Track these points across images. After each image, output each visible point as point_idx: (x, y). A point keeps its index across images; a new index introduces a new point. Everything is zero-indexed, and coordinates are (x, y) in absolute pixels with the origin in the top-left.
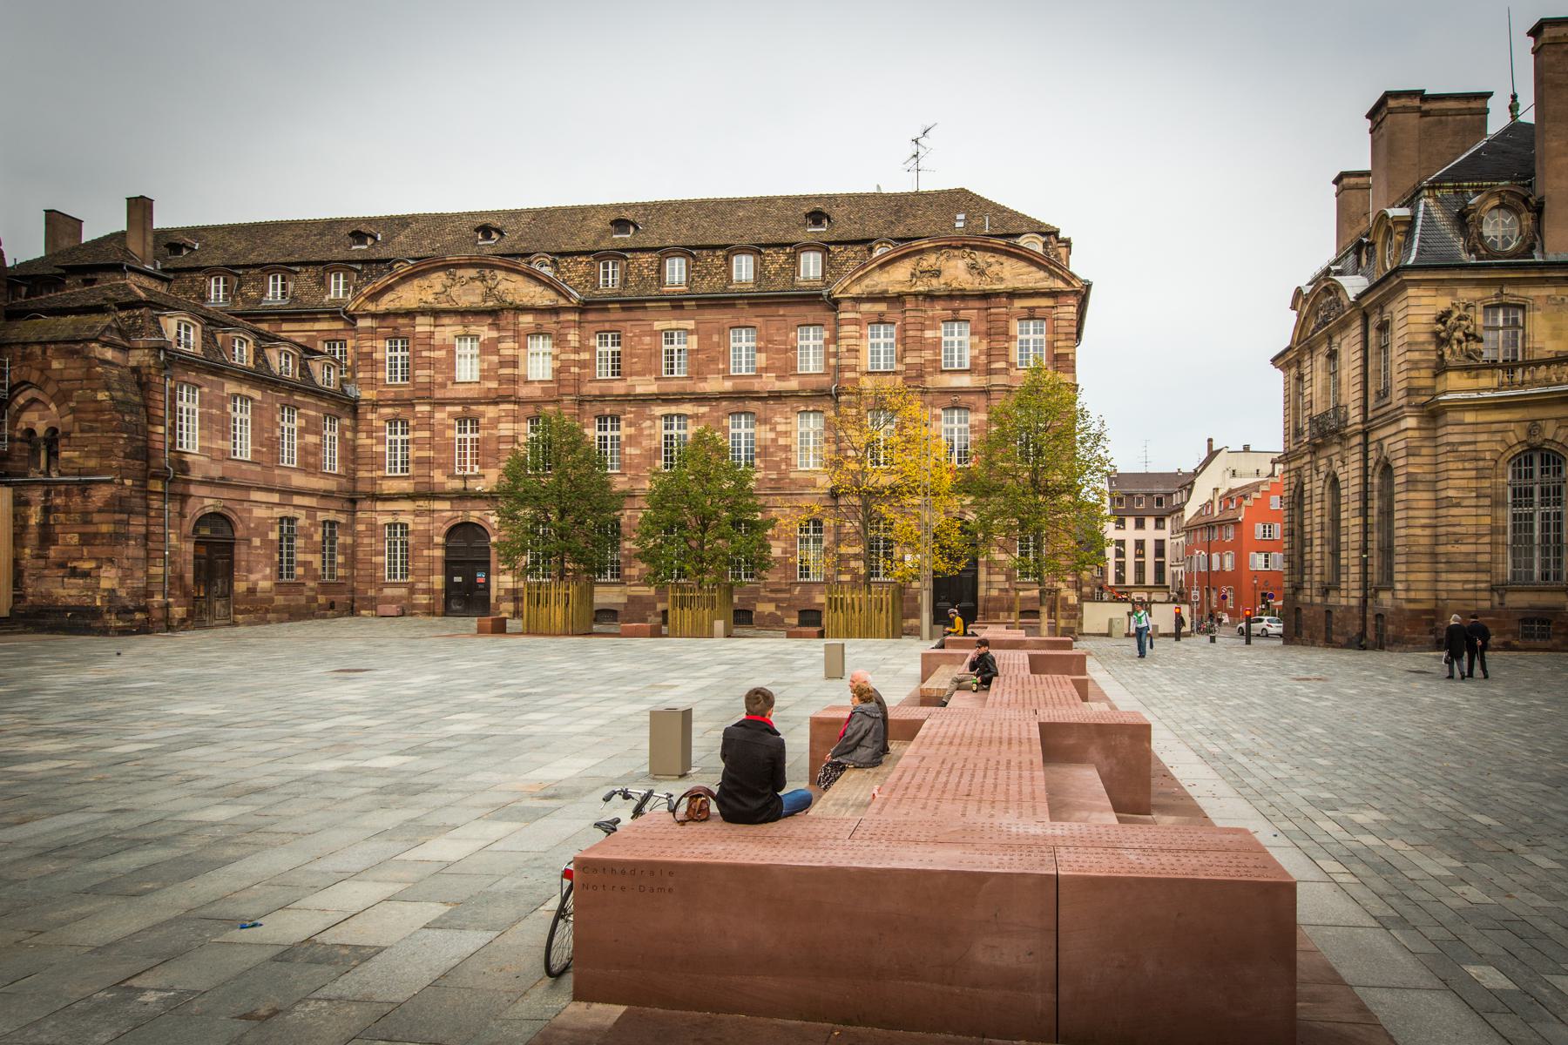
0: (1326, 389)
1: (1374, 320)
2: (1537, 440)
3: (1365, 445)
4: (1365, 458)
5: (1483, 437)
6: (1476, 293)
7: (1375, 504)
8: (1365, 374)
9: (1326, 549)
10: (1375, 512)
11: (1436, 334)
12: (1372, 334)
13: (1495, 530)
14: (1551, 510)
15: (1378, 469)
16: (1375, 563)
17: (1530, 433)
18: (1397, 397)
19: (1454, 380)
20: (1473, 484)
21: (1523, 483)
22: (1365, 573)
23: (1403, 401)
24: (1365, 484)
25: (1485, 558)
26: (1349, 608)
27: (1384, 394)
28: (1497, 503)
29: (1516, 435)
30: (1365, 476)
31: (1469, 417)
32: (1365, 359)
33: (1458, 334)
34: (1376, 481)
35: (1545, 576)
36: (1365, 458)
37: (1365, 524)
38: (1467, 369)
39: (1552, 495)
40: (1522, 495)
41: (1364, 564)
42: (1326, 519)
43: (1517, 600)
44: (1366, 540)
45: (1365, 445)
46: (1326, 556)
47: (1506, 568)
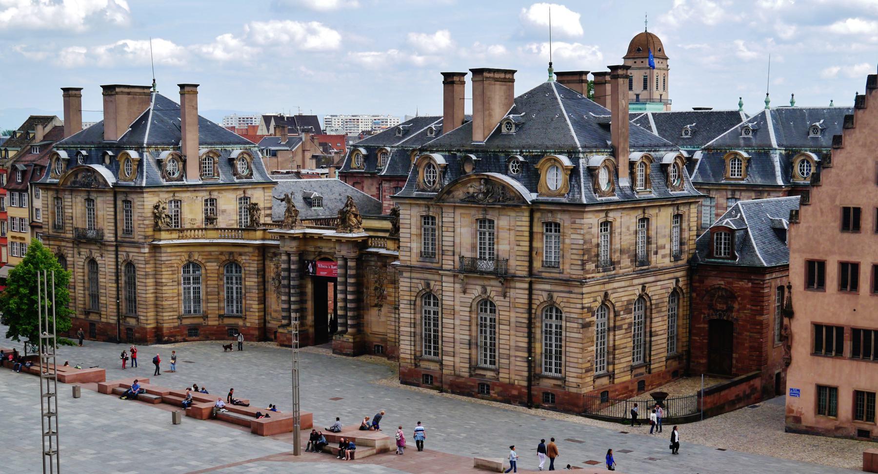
0: (83, 215)
1: (121, 198)
2: (192, 260)
3: (117, 252)
4: (117, 258)
5: (173, 258)
6: (166, 196)
7: (123, 279)
8: (116, 219)
9: (87, 292)
10: (123, 282)
11: (154, 213)
12: (119, 203)
13: (179, 295)
14: (196, 286)
15: (125, 264)
16: (123, 306)
17: (190, 257)
18: (138, 236)
19: (164, 235)
20: (171, 277)
21: (186, 275)
22: (118, 309)
23: (143, 241)
24: (117, 269)
25: (175, 306)
26: (108, 324)
27: (129, 231)
28: (179, 284)
29: (185, 257)
30: (117, 265)
31: (169, 250)
32: (115, 215)
33: (163, 215)
34: (123, 268)
35: (195, 311)
36: (117, 258)
37: (118, 287)
38: (168, 230)
39: (197, 280)
40: (187, 280)
41: (118, 305)
42: (86, 278)
43: (186, 322)
44: (118, 294)
45: (117, 252)
46: (87, 296)
47: (182, 309)
